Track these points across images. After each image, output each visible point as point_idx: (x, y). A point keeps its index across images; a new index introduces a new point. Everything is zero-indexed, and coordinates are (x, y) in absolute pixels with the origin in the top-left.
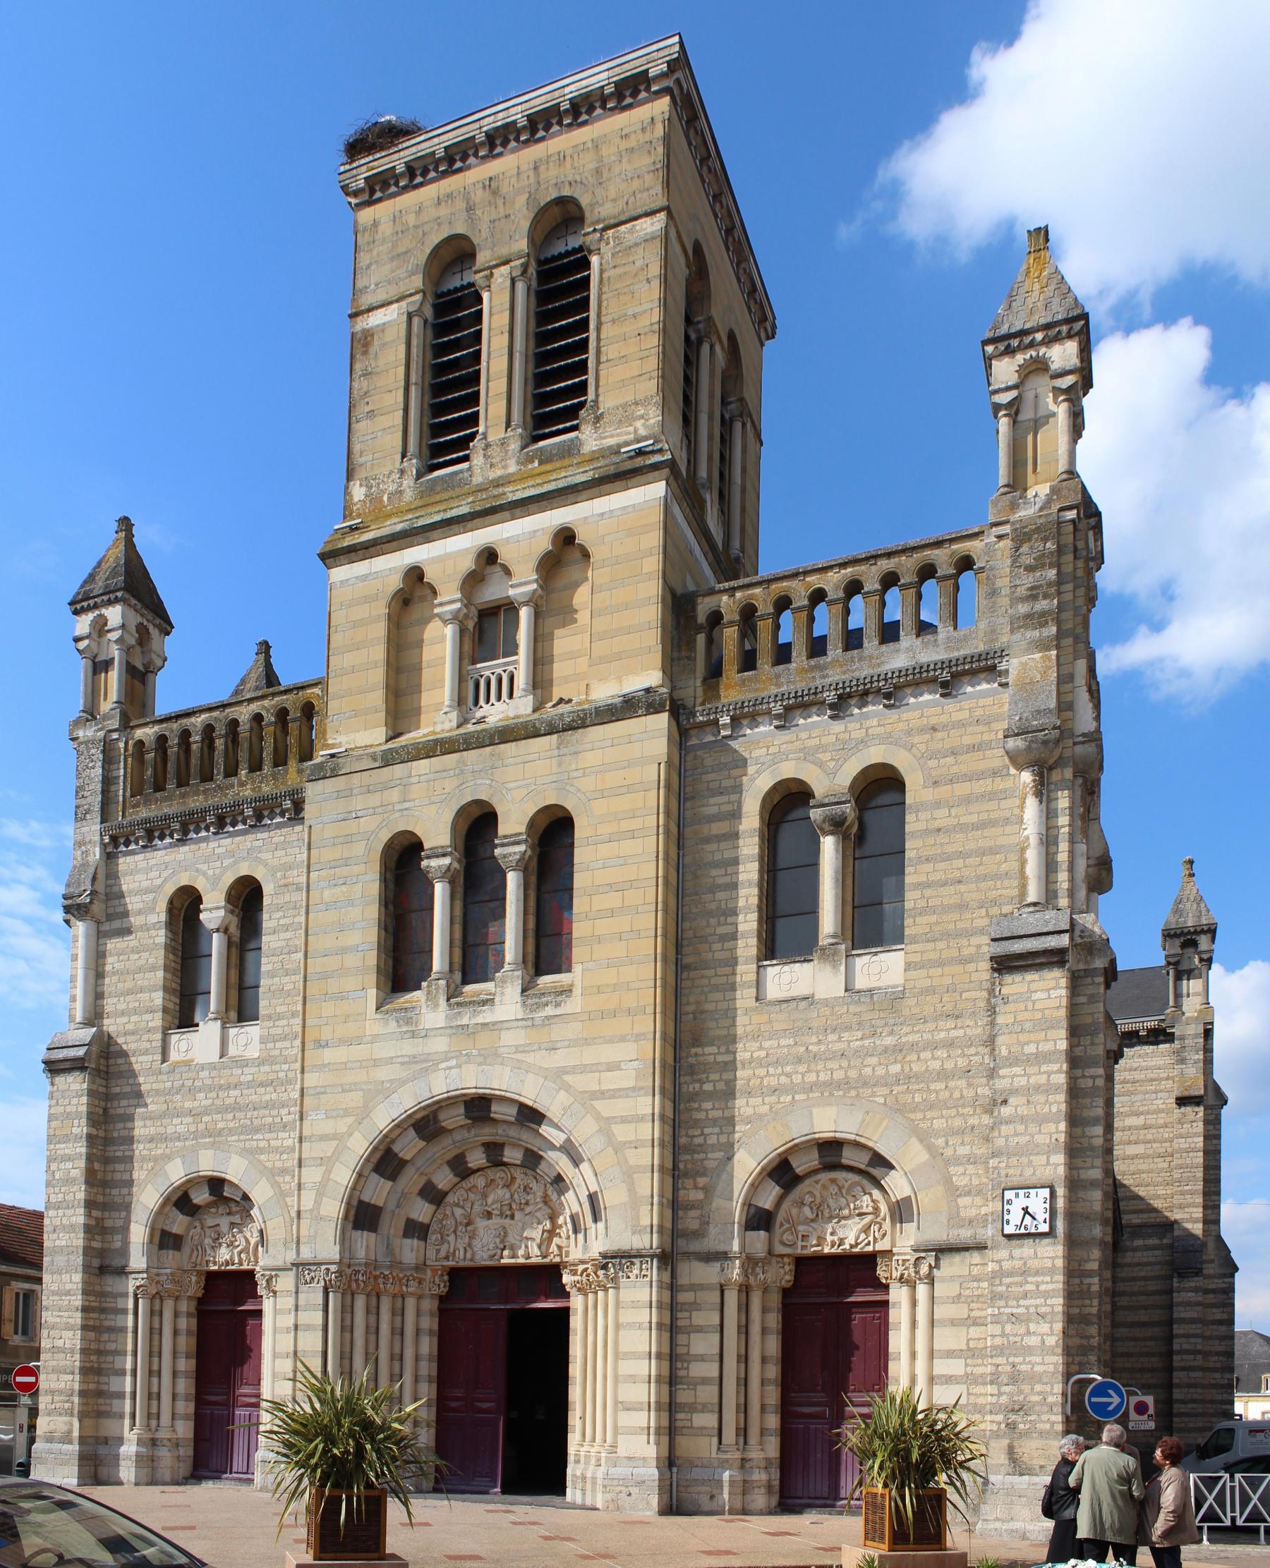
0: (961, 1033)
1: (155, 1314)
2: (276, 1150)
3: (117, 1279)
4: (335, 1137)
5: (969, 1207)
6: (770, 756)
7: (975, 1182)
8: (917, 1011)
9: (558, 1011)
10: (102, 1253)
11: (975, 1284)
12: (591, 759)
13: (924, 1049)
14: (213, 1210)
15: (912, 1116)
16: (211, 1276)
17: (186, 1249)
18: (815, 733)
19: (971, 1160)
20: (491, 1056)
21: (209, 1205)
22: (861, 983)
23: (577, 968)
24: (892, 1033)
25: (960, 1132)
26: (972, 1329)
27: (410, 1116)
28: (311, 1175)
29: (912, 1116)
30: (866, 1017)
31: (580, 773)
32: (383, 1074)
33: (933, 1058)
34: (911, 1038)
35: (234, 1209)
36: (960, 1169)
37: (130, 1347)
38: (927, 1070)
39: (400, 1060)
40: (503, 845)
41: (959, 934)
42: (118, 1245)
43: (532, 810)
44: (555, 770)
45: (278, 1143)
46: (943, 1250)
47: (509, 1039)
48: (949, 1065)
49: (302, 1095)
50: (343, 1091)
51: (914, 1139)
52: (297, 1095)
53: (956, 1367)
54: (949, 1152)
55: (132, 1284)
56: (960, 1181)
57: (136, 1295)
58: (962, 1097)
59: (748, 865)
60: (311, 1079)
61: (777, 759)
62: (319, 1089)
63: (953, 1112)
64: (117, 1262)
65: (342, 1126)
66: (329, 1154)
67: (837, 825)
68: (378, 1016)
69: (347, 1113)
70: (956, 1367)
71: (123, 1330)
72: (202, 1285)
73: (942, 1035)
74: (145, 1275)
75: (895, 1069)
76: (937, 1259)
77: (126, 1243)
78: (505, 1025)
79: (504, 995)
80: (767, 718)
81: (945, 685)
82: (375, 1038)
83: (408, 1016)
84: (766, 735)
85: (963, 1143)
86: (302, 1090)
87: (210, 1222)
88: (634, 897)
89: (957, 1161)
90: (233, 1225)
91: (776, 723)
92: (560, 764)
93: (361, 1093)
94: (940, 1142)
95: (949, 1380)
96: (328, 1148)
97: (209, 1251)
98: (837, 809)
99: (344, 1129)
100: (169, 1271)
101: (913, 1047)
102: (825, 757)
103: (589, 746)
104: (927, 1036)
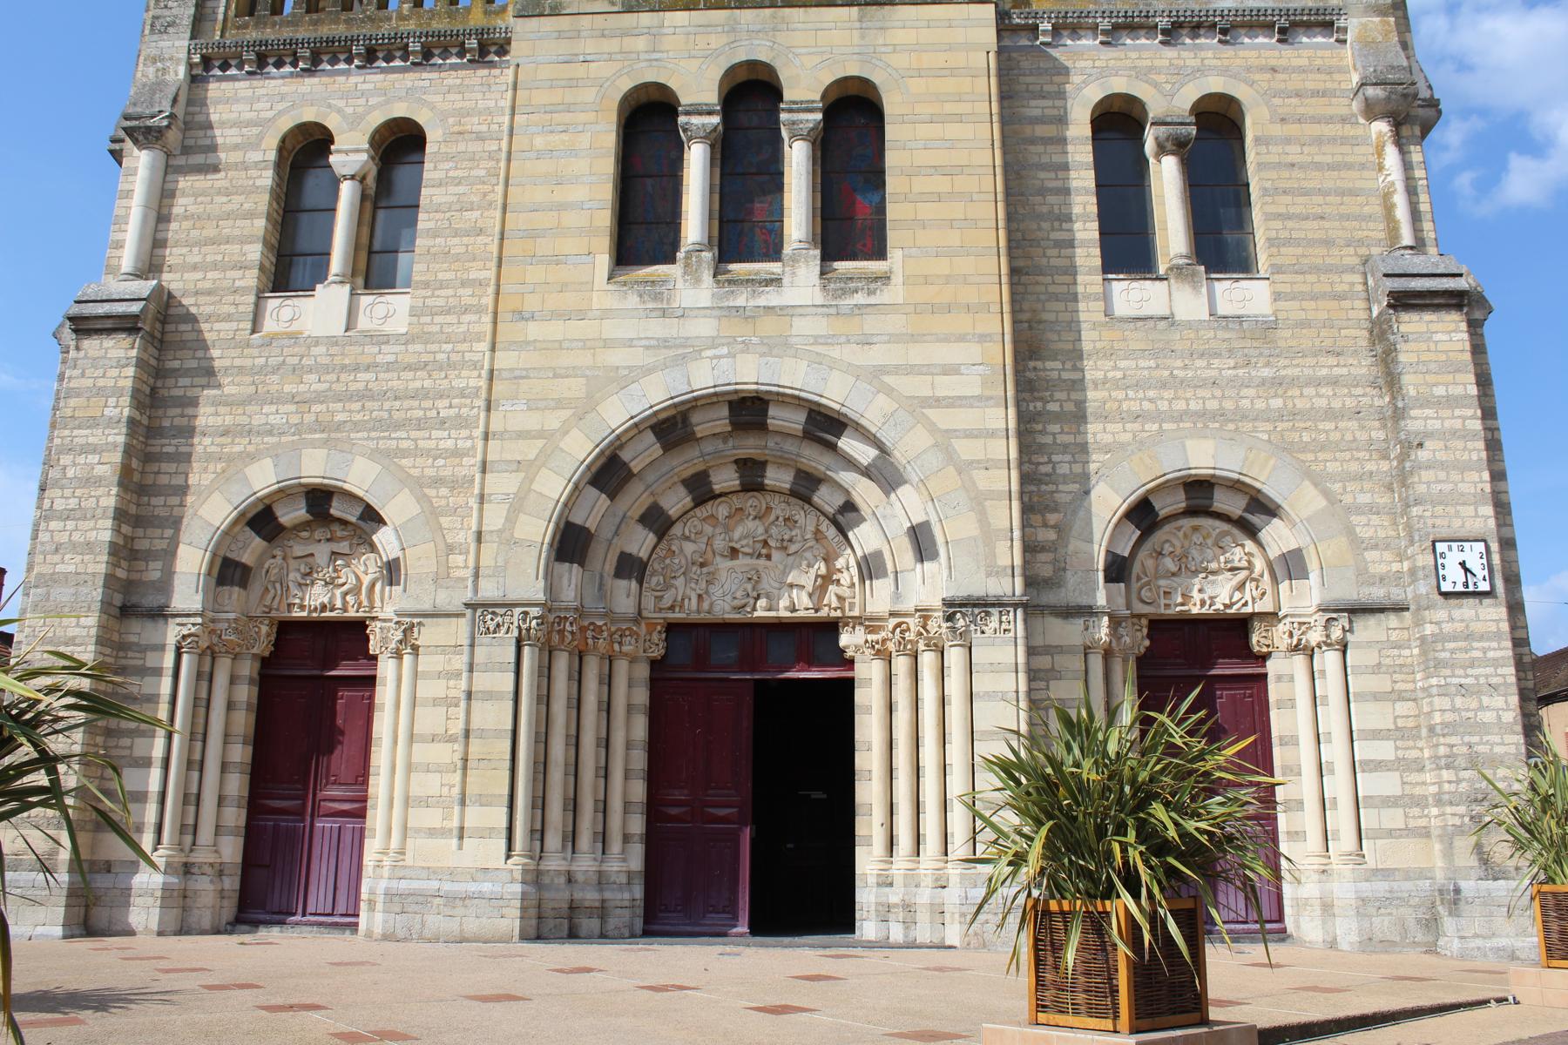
0: (1344, 371)
1: (204, 677)
2: (427, 453)
3: (149, 624)
4: (541, 434)
5: (1380, 562)
6: (1092, 73)
7: (1381, 534)
8: (1294, 343)
9: (872, 300)
10: (129, 586)
11: (1396, 652)
12: (900, 36)
13: (1307, 385)
14: (305, 534)
15: (1302, 456)
16: (287, 629)
17: (256, 587)
18: (1145, 54)
19: (1373, 509)
20: (779, 346)
21: (304, 526)
22: (1222, 310)
23: (895, 255)
24: (1268, 364)
25: (1359, 477)
26: (1398, 705)
27: (656, 413)
28: (502, 484)
29: (1302, 456)
30: (1236, 344)
31: (890, 49)
32: (617, 357)
33: (1318, 395)
34: (1289, 372)
35: (339, 534)
36: (1363, 519)
38: (1312, 408)
39: (644, 343)
40: (790, 111)
41: (1329, 270)
42: (155, 575)
43: (828, 79)
44: (856, 41)
45: (432, 444)
46: (1357, 611)
47: (803, 327)
48: (1336, 404)
49: (491, 379)
50: (555, 376)
51: (1307, 483)
52: (483, 383)
53: (1384, 750)
54: (1348, 499)
55: (172, 633)
56: (1364, 533)
58: (1355, 440)
59: (1083, 173)
60: (504, 360)
61: (1104, 73)
62: (517, 373)
63: (1347, 455)
64: (151, 601)
65: (553, 421)
66: (531, 457)
67: (1178, 146)
68: (611, 287)
69: (559, 404)
70: (1384, 750)
71: (153, 699)
72: (273, 639)
73: (1324, 372)
74: (199, 620)
75: (1277, 403)
76: (1351, 622)
77: (169, 573)
78: (800, 311)
79: (799, 277)
80: (1090, 33)
81: (1282, 31)
82: (606, 314)
83: (655, 290)
84: (1089, 48)
85: (1361, 490)
86: (492, 371)
87: (299, 550)
88: (964, 183)
89: (1359, 510)
90: (335, 555)
91: (1101, 38)
92: (863, 37)
93: (583, 381)
94: (1337, 487)
95: (1377, 766)
96: (531, 450)
97: (294, 590)
98: (1183, 130)
99: (556, 425)
100: (232, 616)
101: (1294, 381)
102: (1162, 78)
103: (899, 24)
104: (1306, 371)
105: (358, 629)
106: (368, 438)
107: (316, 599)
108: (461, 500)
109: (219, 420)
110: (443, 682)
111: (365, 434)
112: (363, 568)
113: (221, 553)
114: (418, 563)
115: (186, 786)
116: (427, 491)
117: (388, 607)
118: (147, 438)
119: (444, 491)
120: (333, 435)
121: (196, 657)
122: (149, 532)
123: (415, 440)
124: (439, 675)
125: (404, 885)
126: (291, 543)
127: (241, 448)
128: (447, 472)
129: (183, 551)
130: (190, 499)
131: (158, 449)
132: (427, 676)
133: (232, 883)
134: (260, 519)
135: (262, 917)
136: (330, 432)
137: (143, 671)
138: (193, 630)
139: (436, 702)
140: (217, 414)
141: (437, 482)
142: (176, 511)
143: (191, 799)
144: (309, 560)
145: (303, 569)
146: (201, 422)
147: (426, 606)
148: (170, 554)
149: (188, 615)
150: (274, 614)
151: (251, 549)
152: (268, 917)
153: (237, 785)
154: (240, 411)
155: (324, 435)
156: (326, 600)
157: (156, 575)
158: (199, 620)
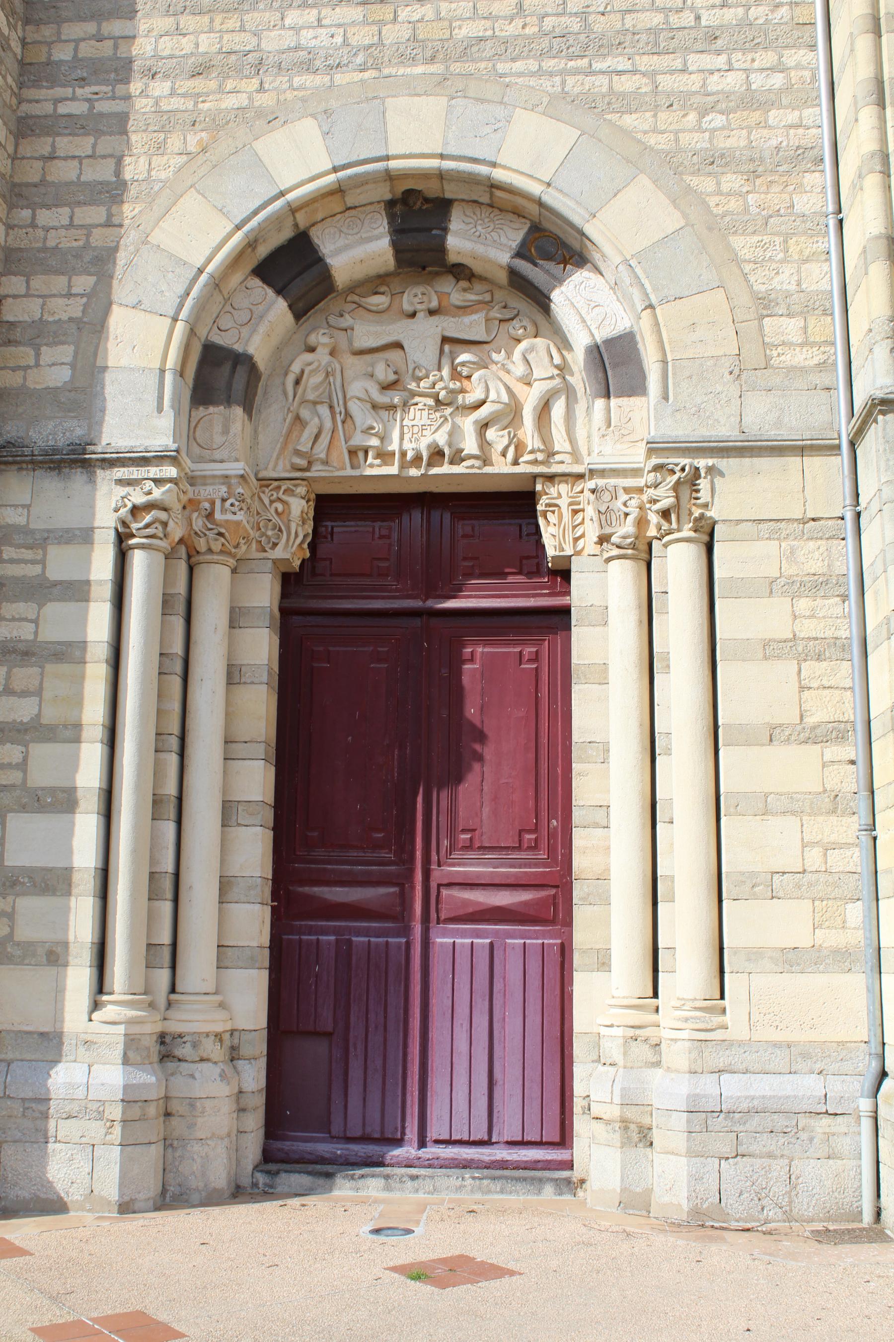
1: (179, 607)
2: (677, 102)
3: (50, 485)
14: (379, 301)
17: (274, 415)
21: (376, 283)
37: (94, 712)
45: (693, 82)
55: (108, 501)
57: (122, 539)
64: (51, 432)
71: (70, 653)
74: (171, 471)
87: (367, 333)
100: (236, 468)
105: (516, 505)
106: (539, 73)
107: (414, 440)
108: (775, 199)
109: (187, 44)
110: (780, 605)
111: (533, 65)
112: (519, 369)
113: (202, 332)
114: (687, 334)
115: (153, 861)
116: (694, 181)
117: (610, 437)
118: (21, 86)
119: (732, 181)
120: (456, 68)
121: (160, 557)
122: (38, 283)
123: (651, 75)
124: (771, 587)
125: (733, 1087)
126: (347, 321)
127: (242, 100)
128: (736, 141)
129: (120, 320)
130: (129, 210)
131: (48, 108)
132: (744, 589)
133: (254, 1076)
134: (289, 264)
135: (324, 1148)
136: (450, 62)
137: (42, 590)
138: (158, 493)
139: (770, 649)
140: (179, 32)
141: (714, 161)
142: (98, 238)
143: (169, 887)
144: (394, 355)
145: (383, 373)
146: (143, 48)
147: (724, 429)
148: (92, 327)
149: (144, 461)
150: (318, 471)
151: (264, 325)
152: (339, 1149)
153: (254, 851)
154: (233, 23)
155: (436, 68)
156: (441, 438)
157: (60, 376)
158: (171, 471)
